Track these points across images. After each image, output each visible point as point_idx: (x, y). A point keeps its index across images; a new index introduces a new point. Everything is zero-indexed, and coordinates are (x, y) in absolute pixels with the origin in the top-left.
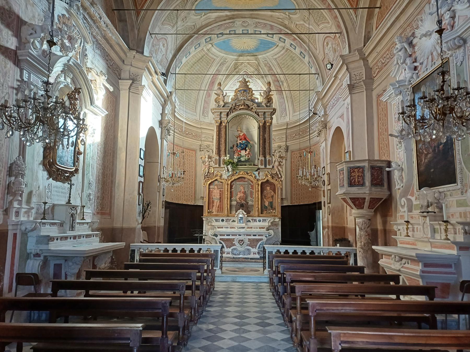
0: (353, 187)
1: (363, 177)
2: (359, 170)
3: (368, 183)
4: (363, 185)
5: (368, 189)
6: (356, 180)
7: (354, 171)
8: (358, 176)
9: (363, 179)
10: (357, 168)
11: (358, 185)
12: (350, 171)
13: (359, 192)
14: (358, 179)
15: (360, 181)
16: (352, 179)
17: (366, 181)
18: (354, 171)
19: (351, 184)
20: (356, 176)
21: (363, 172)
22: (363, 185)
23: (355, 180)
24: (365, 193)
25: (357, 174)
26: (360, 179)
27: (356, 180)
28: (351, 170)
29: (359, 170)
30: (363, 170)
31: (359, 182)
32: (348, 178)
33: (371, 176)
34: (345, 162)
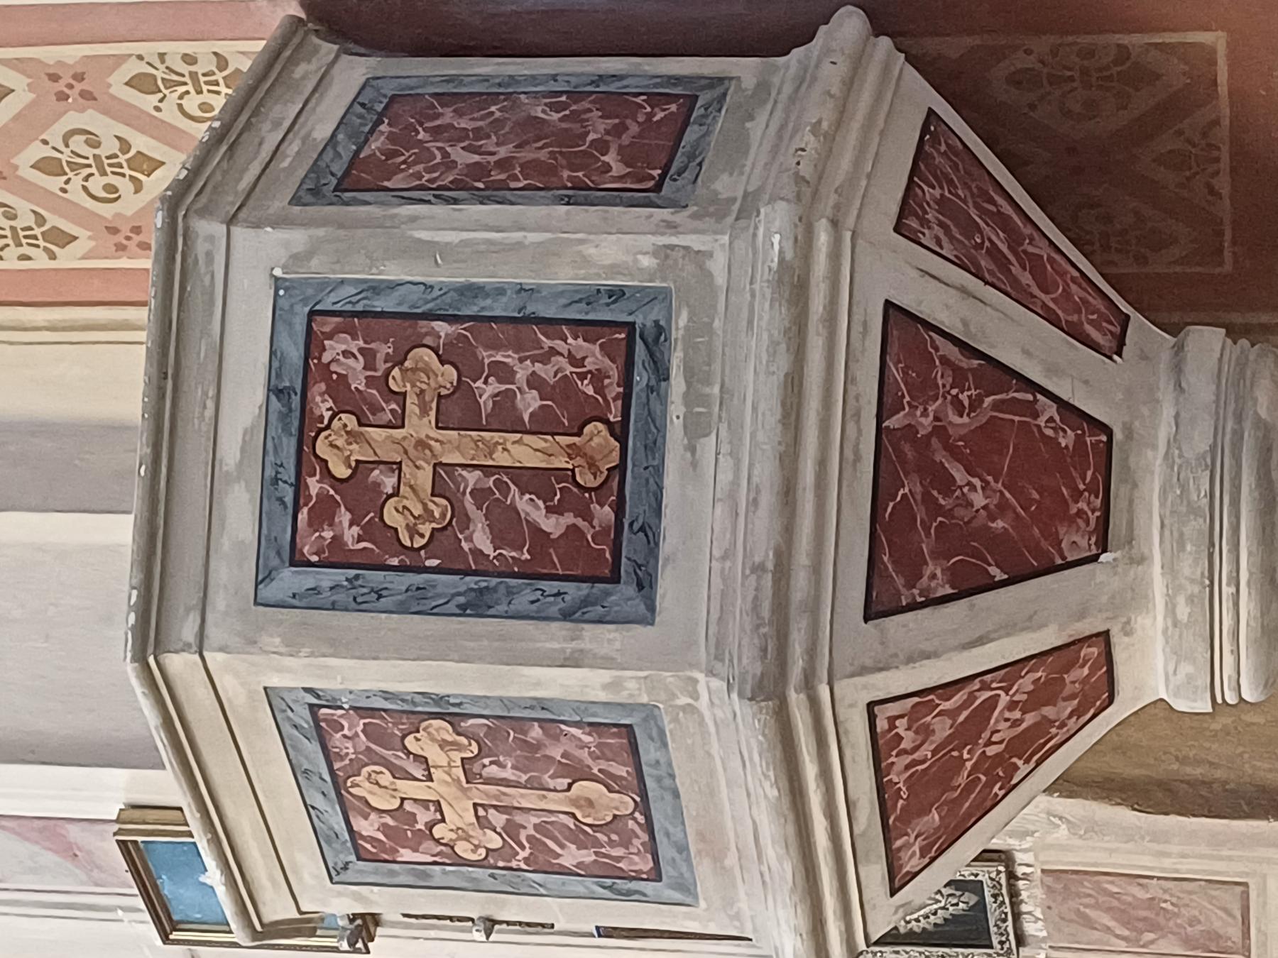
0: (650, 534)
1: (481, 327)
2: (345, 399)
3: (608, 248)
4: (630, 338)
5: (715, 245)
6: (525, 452)
7: (359, 490)
8: (457, 411)
9: (526, 325)
10: (306, 431)
11: (635, 429)
12: (335, 558)
13: (756, 384)
14: (506, 419)
15: (562, 391)
16: (507, 527)
17: (564, 275)
18: (359, 490)
19: (595, 558)
20: (455, 447)
21: (389, 323)
22: (630, 338)
23: (535, 480)
24: (793, 283)
25: (420, 425)
26: (524, 379)
27: (525, 452)
28: (336, 542)
29: (345, 399)
30: (357, 319)
31: (566, 412)
32: (476, 606)
33: (494, 193)
34: (150, 637)
